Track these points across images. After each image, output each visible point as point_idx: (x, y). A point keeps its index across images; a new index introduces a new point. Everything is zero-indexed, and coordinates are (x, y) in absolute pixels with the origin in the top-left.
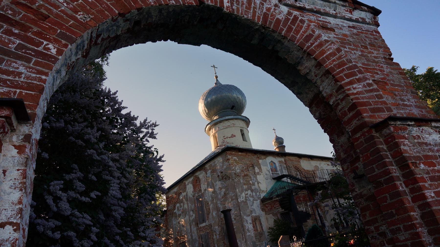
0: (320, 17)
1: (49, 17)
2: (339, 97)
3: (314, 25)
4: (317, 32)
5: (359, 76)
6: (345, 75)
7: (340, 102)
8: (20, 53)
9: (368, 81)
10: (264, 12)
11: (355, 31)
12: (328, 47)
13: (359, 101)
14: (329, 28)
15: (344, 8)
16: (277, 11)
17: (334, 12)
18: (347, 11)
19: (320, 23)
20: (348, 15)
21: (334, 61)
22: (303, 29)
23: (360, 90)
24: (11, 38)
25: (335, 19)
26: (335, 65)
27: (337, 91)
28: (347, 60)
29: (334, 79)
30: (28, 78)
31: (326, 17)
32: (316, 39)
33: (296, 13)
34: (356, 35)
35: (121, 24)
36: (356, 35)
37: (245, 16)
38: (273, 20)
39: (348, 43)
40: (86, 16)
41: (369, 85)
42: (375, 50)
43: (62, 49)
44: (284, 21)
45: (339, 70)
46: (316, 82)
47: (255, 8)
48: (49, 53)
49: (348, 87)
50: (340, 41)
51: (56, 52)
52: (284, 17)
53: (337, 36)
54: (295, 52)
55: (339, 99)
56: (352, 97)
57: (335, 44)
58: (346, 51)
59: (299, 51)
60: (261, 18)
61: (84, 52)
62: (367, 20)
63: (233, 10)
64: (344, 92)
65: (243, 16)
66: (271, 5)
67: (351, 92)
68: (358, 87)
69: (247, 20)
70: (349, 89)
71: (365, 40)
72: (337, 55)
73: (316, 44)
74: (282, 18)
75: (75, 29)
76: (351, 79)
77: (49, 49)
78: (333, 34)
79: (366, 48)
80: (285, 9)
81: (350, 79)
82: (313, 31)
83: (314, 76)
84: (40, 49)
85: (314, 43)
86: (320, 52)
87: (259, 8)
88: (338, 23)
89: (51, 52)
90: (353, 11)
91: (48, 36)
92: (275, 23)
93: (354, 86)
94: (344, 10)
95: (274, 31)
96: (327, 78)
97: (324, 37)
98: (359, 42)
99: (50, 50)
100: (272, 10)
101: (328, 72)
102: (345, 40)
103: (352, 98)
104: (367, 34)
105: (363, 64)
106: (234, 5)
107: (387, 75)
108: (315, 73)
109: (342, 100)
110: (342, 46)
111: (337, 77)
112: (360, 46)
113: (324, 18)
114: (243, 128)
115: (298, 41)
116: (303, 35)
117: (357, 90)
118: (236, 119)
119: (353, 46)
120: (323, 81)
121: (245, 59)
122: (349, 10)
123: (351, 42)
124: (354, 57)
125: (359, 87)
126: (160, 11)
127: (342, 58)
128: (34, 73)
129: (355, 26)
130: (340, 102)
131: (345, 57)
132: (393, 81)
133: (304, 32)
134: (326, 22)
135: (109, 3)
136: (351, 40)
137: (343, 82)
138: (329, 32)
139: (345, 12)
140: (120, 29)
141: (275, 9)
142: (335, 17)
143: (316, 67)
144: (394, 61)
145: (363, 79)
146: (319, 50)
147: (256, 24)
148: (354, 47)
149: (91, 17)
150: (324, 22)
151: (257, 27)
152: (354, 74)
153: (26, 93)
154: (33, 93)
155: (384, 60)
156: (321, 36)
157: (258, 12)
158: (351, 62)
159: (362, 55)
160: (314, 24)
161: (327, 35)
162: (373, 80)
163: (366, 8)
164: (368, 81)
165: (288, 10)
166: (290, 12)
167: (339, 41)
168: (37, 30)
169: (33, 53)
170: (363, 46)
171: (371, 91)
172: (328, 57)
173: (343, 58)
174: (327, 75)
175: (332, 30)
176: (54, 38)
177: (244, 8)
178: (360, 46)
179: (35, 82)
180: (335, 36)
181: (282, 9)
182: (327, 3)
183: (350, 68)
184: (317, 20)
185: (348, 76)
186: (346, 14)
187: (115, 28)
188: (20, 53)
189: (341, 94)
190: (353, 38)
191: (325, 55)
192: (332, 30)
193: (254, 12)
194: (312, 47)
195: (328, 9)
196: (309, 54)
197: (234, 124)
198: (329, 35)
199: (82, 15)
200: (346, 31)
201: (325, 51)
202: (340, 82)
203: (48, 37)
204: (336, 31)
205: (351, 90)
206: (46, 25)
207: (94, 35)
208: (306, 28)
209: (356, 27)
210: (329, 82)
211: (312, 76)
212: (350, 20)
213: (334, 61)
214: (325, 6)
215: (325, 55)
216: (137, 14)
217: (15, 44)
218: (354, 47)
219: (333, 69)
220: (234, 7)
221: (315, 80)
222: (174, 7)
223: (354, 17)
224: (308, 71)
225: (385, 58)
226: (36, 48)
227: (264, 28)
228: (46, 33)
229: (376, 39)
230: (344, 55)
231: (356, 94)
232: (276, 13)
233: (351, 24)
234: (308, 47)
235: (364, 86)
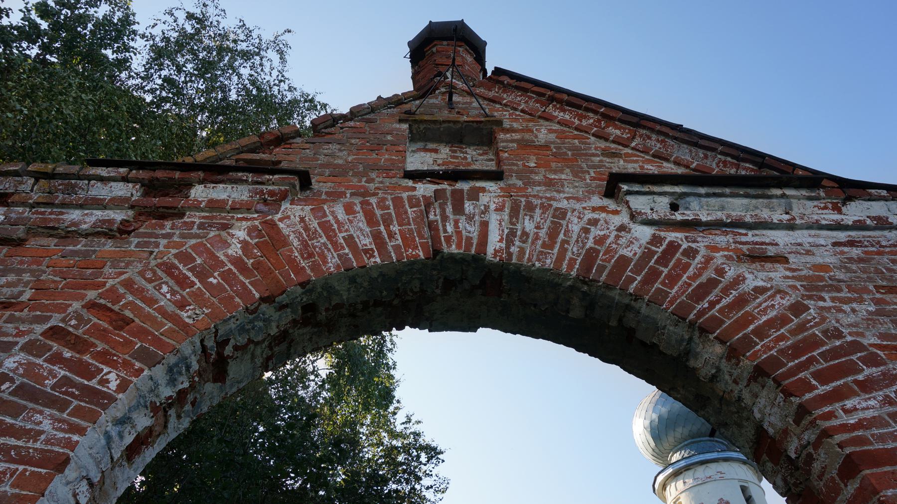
0: (746, 235)
1: (133, 321)
2: (806, 437)
3: (725, 256)
4: (731, 273)
6: (817, 375)
7: (812, 451)
8: (57, 394)
10: (587, 247)
11: (855, 252)
12: (764, 305)
13: (865, 448)
14: (771, 257)
15: (816, 203)
16: (622, 241)
17: (787, 217)
18: (825, 208)
19: (745, 248)
20: (832, 217)
21: (782, 338)
22: (691, 269)
24: (55, 368)
25: (791, 233)
26: (781, 352)
27: (797, 422)
28: (825, 332)
29: (780, 388)
31: (764, 232)
32: (726, 291)
33: (672, 236)
34: (860, 260)
35: (271, 316)
37: (537, 263)
38: (609, 262)
39: (831, 285)
40: (197, 312)
43: (130, 378)
44: (638, 260)
45: (796, 361)
46: (739, 397)
48: (105, 389)
49: (827, 409)
50: (805, 283)
51: (117, 386)
52: (639, 252)
53: (795, 274)
54: (671, 328)
55: (809, 443)
56: (838, 438)
57: (787, 293)
58: (822, 308)
59: (677, 325)
60: (578, 262)
61: (193, 377)
63: (510, 255)
64: (813, 423)
65: (534, 265)
66: (608, 229)
67: (835, 422)
68: (864, 405)
70: (831, 415)
72: (793, 321)
74: (635, 254)
75: (168, 338)
76: (838, 383)
78: (782, 269)
80: (644, 233)
81: (834, 384)
82: (720, 272)
83: (730, 382)
84: (93, 383)
85: (718, 302)
86: (736, 321)
87: (577, 241)
88: (799, 241)
89: (108, 387)
90: (844, 204)
91: (115, 358)
92: (614, 267)
93: (849, 404)
94: (815, 206)
95: (607, 286)
96: (763, 387)
98: (870, 279)
99: (109, 382)
102: (822, 279)
103: (841, 442)
105: (882, 336)
106: (514, 245)
108: (731, 375)
109: (817, 444)
110: (810, 297)
111: (787, 382)
112: (871, 287)
113: (757, 235)
114: (746, 481)
115: (671, 303)
116: (690, 285)
117: (861, 415)
118: (726, 460)
119: (849, 292)
120: (756, 396)
121: (579, 349)
122: (830, 206)
123: (839, 281)
126: (353, 280)
127: (807, 329)
128: (64, 431)
129: (858, 239)
130: (812, 451)
131: (816, 325)
134: (762, 243)
135: (247, 282)
136: (840, 275)
137: (808, 396)
138: (768, 265)
139: (821, 211)
140: (274, 325)
141: (617, 237)
142: (791, 226)
143: (729, 359)
145: (884, 380)
146: (734, 315)
147: (566, 277)
148: (849, 295)
149: (206, 311)
150: (757, 243)
151: (569, 283)
152: (852, 369)
153: (33, 472)
154: (43, 471)
156: (744, 279)
157: (573, 249)
159: (878, 313)
160: (726, 253)
161: (763, 275)
163: (884, 193)
165: (653, 232)
166: (660, 237)
167: (801, 286)
168: (104, 349)
169: (77, 393)
170: (883, 287)
172: (760, 333)
173: (812, 327)
174: (760, 378)
175: (781, 259)
176: (124, 360)
177: (538, 247)
178: (871, 287)
179: (56, 449)
180: (788, 273)
181: (636, 235)
182: (761, 200)
183: (834, 353)
184: (735, 242)
185: (823, 377)
186: (822, 216)
187: (260, 324)
188: (57, 394)
189: (807, 429)
190: (849, 270)
191: (751, 327)
192: (781, 259)
193: (563, 251)
194: (714, 312)
195: (765, 214)
196: (704, 331)
197: (721, 473)
198: (770, 273)
199: (192, 310)
201: (752, 315)
202: (796, 396)
203: (115, 360)
204: (791, 261)
205: (836, 417)
206: (118, 337)
207: (210, 343)
208: (699, 266)
209: (860, 242)
210: (772, 396)
211: (727, 383)
212: (838, 227)
213: (782, 338)
214: (757, 208)
215: (751, 327)
216: (303, 293)
217: (55, 377)
218: (849, 295)
219: (774, 362)
221: (736, 392)
222: (380, 268)
223: (849, 220)
224: (714, 371)
226: (86, 382)
227: (584, 282)
228: (114, 352)
230: (814, 318)
231: (859, 425)
232: (618, 244)
233: (842, 236)
234: (702, 313)
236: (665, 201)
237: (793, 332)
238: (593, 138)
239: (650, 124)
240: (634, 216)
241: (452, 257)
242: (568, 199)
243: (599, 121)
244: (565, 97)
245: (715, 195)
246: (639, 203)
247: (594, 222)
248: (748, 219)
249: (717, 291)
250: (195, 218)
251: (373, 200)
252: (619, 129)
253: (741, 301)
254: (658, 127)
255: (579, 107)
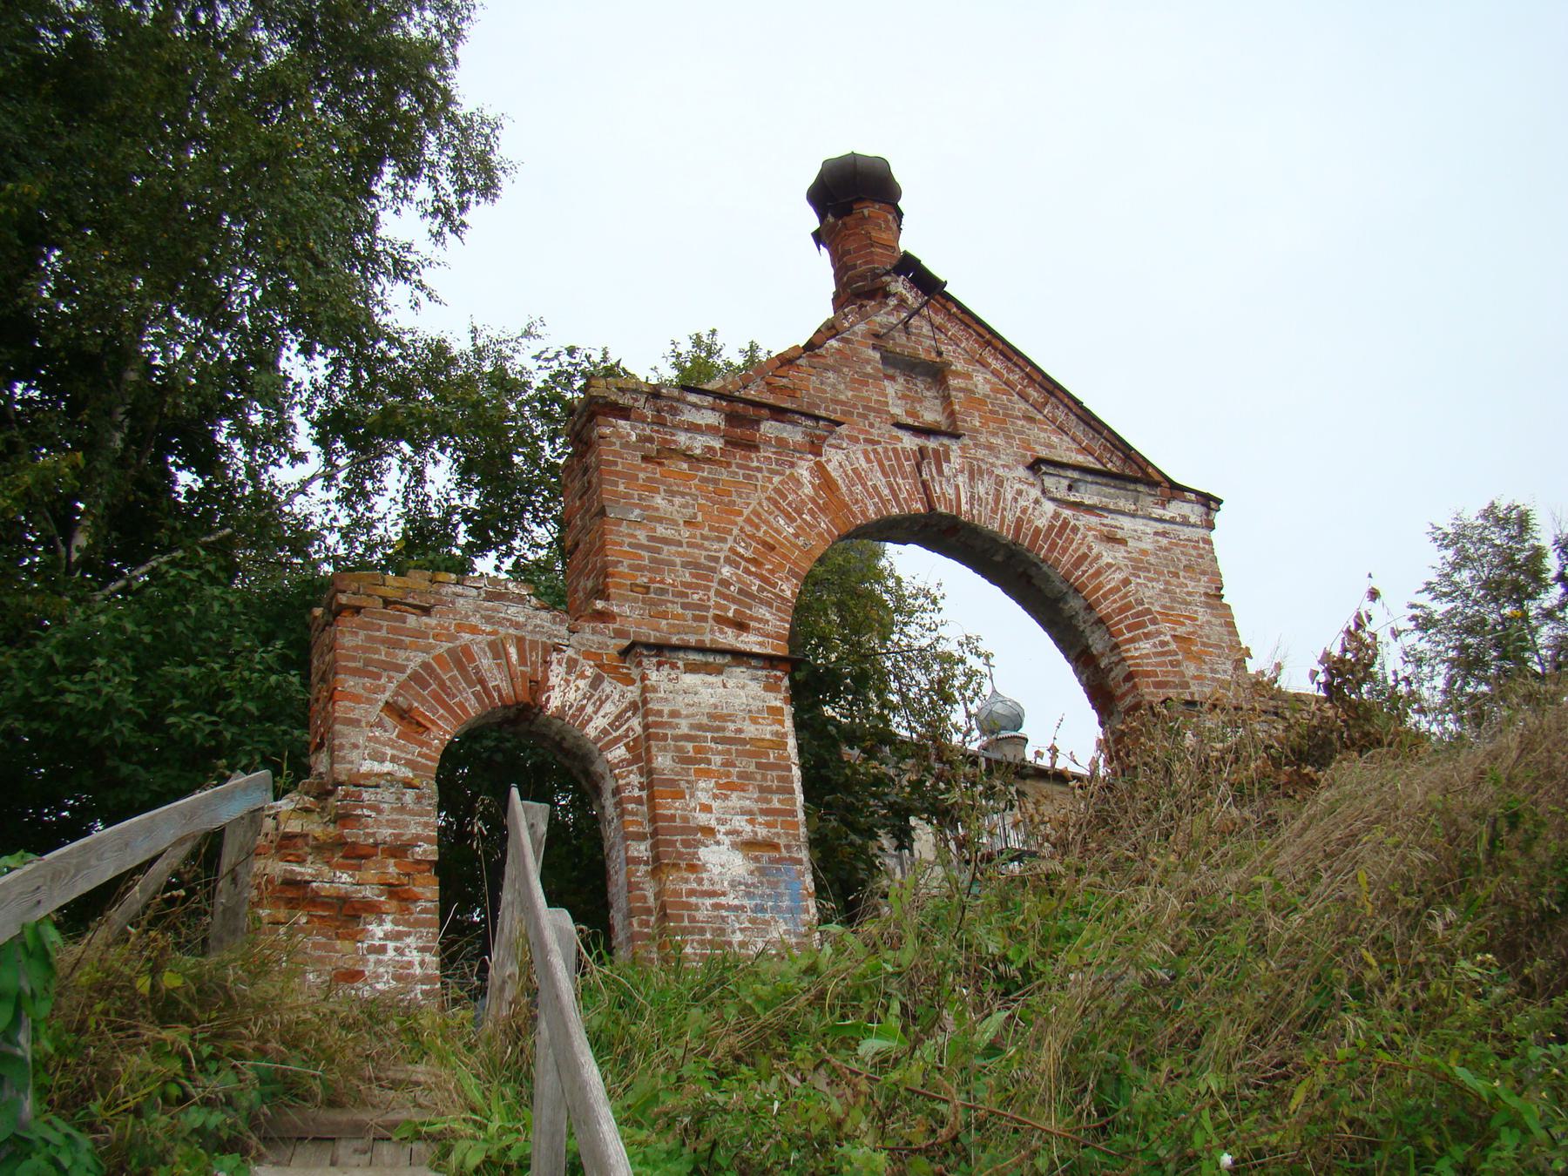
4: (1095, 551)
5: (1151, 628)
9: (1162, 638)
11: (1164, 542)
16: (1036, 513)
17: (1133, 507)
20: (1158, 512)
21: (1115, 601)
23: (1144, 652)
26: (1113, 610)
27: (1111, 650)
30: (775, 626)
33: (1067, 513)
34: (1166, 549)
36: (1166, 549)
41: (1163, 644)
42: (1192, 579)
47: (1004, 509)
62: (1192, 520)
63: (973, 516)
64: (1119, 654)
67: (1129, 654)
69: (992, 531)
70: (1128, 650)
71: (1179, 559)
73: (1090, 572)
77: (783, 591)
79: (1176, 575)
80: (1049, 507)
82: (1090, 548)
84: (777, 590)
95: (1028, 550)
97: (1107, 558)
98: (1167, 566)
100: (1030, 511)
101: (1101, 621)
104: (1185, 546)
107: (1201, 627)
109: (1117, 664)
110: (1134, 575)
124: (1148, 594)
125: (1146, 646)
132: (1208, 638)
133: (1075, 551)
136: (1152, 560)
141: (1034, 509)
143: (1086, 609)
144: (1224, 601)
147: (1004, 538)
152: (1142, 625)
155: (1203, 599)
157: (1009, 516)
158: (1142, 604)
159: (1166, 591)
162: (1174, 637)
164: (1162, 638)
171: (1163, 654)
172: (1105, 597)
175: (1123, 542)
183: (1137, 615)
185: (1130, 628)
192: (1123, 542)
193: (1003, 518)
196: (1077, 591)
200: (1147, 545)
212: (1160, 520)
213: (1115, 601)
219: (1109, 616)
220: (975, 512)
223: (1167, 514)
225: (1206, 594)
229: (1201, 556)
233: (1160, 527)
234: (1077, 579)
235: (1154, 646)
236: (1065, 483)
237: (1122, 598)
238: (1016, 396)
239: (1061, 395)
240: (1044, 492)
241: (941, 514)
242: (1003, 466)
243: (1023, 379)
244: (1001, 346)
245: (1097, 483)
246: (1049, 482)
247: (1020, 492)
248: (1111, 507)
249: (1086, 563)
250: (767, 452)
251: (880, 450)
252: (1038, 392)
253: (1098, 573)
254: (1066, 400)
255: (1010, 360)
